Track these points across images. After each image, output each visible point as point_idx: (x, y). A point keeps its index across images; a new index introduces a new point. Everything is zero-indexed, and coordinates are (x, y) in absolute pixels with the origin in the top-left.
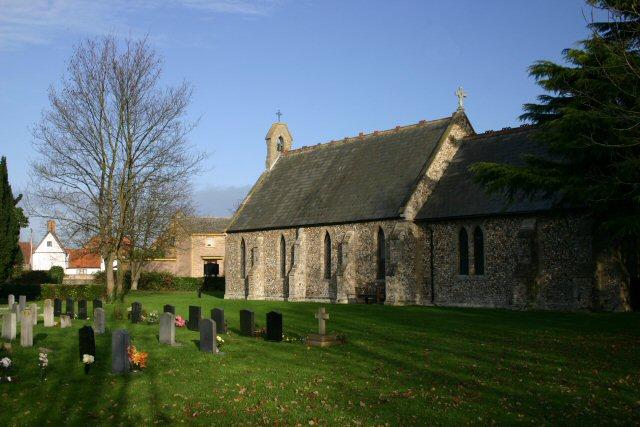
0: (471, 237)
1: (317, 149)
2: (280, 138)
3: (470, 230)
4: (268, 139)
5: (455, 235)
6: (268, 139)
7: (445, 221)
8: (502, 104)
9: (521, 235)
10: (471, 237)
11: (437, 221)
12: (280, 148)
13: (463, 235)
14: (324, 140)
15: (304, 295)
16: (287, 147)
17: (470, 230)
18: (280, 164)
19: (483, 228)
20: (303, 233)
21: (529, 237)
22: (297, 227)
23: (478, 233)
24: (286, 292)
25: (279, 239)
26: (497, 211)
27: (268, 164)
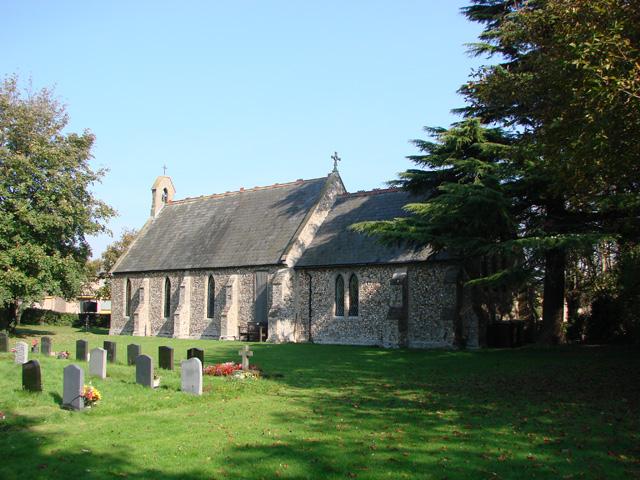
0: (346, 283)
1: (200, 200)
2: (165, 190)
3: (346, 277)
4: (154, 191)
5: (332, 280)
6: (154, 191)
7: (323, 268)
8: (378, 159)
9: (394, 282)
10: (346, 283)
11: (317, 268)
12: (165, 199)
13: (339, 279)
14: (207, 193)
15: (188, 333)
16: (171, 197)
17: (346, 277)
18: (164, 214)
19: (359, 276)
20: (188, 280)
21: (402, 283)
22: (180, 272)
23: (353, 278)
24: (129, 281)
25: (164, 280)
26: (372, 261)
27: (153, 213)
